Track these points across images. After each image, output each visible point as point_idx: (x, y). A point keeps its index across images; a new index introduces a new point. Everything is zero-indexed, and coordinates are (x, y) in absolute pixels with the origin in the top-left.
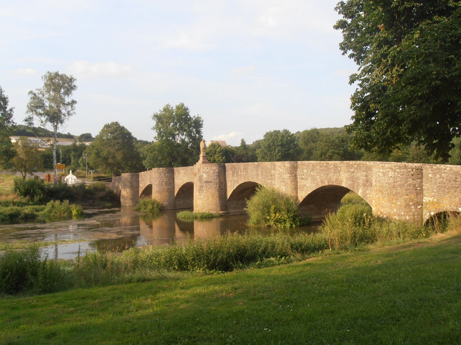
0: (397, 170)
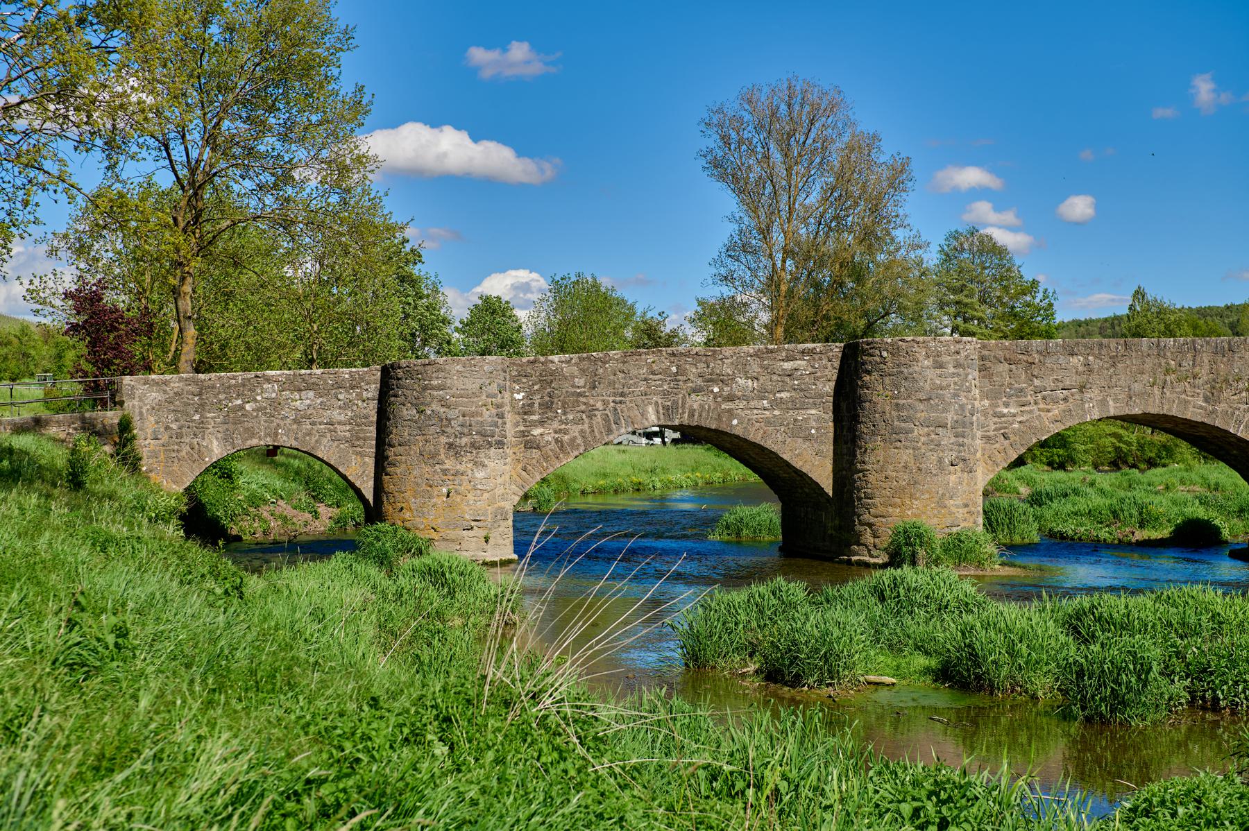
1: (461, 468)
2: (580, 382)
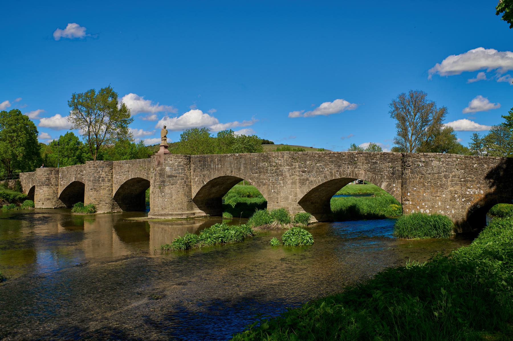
0: (442, 159)
1: (38, 190)
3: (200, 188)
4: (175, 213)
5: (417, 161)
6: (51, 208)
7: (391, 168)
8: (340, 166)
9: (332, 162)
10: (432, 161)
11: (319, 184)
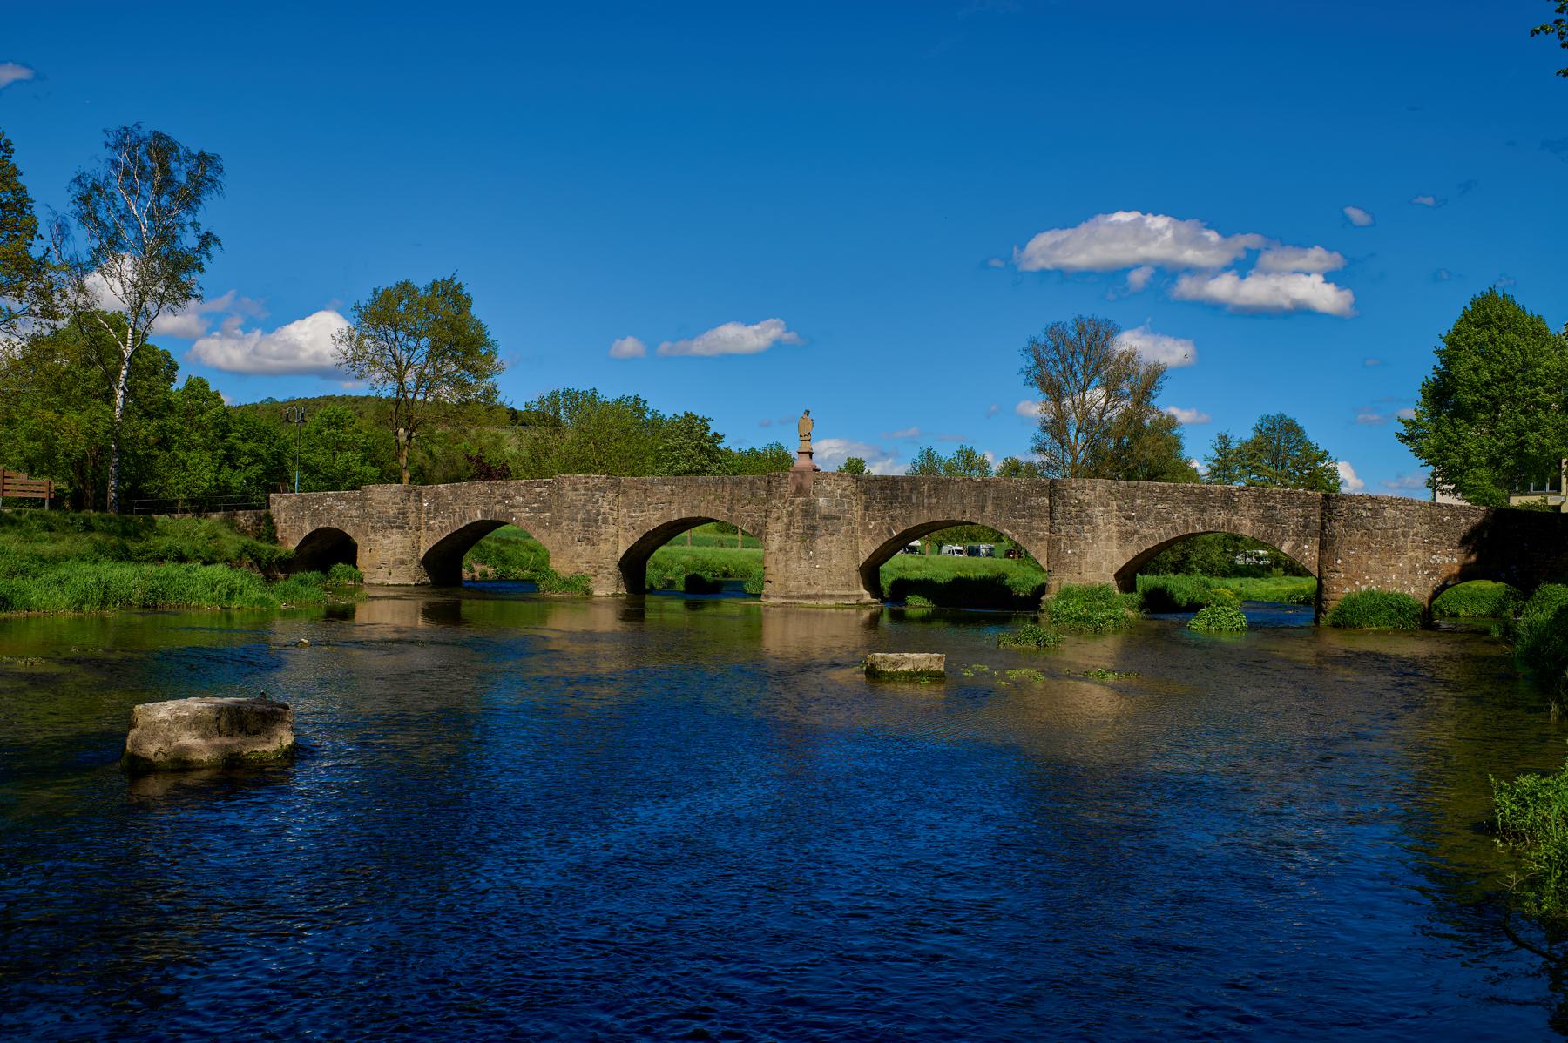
0: (1400, 507)
1: (377, 538)
2: (450, 498)
3: (881, 543)
4: (836, 592)
5: (1358, 508)
6: (407, 585)
7: (1302, 517)
8: (1203, 511)
9: (1188, 502)
10: (1384, 508)
11: (1159, 542)
